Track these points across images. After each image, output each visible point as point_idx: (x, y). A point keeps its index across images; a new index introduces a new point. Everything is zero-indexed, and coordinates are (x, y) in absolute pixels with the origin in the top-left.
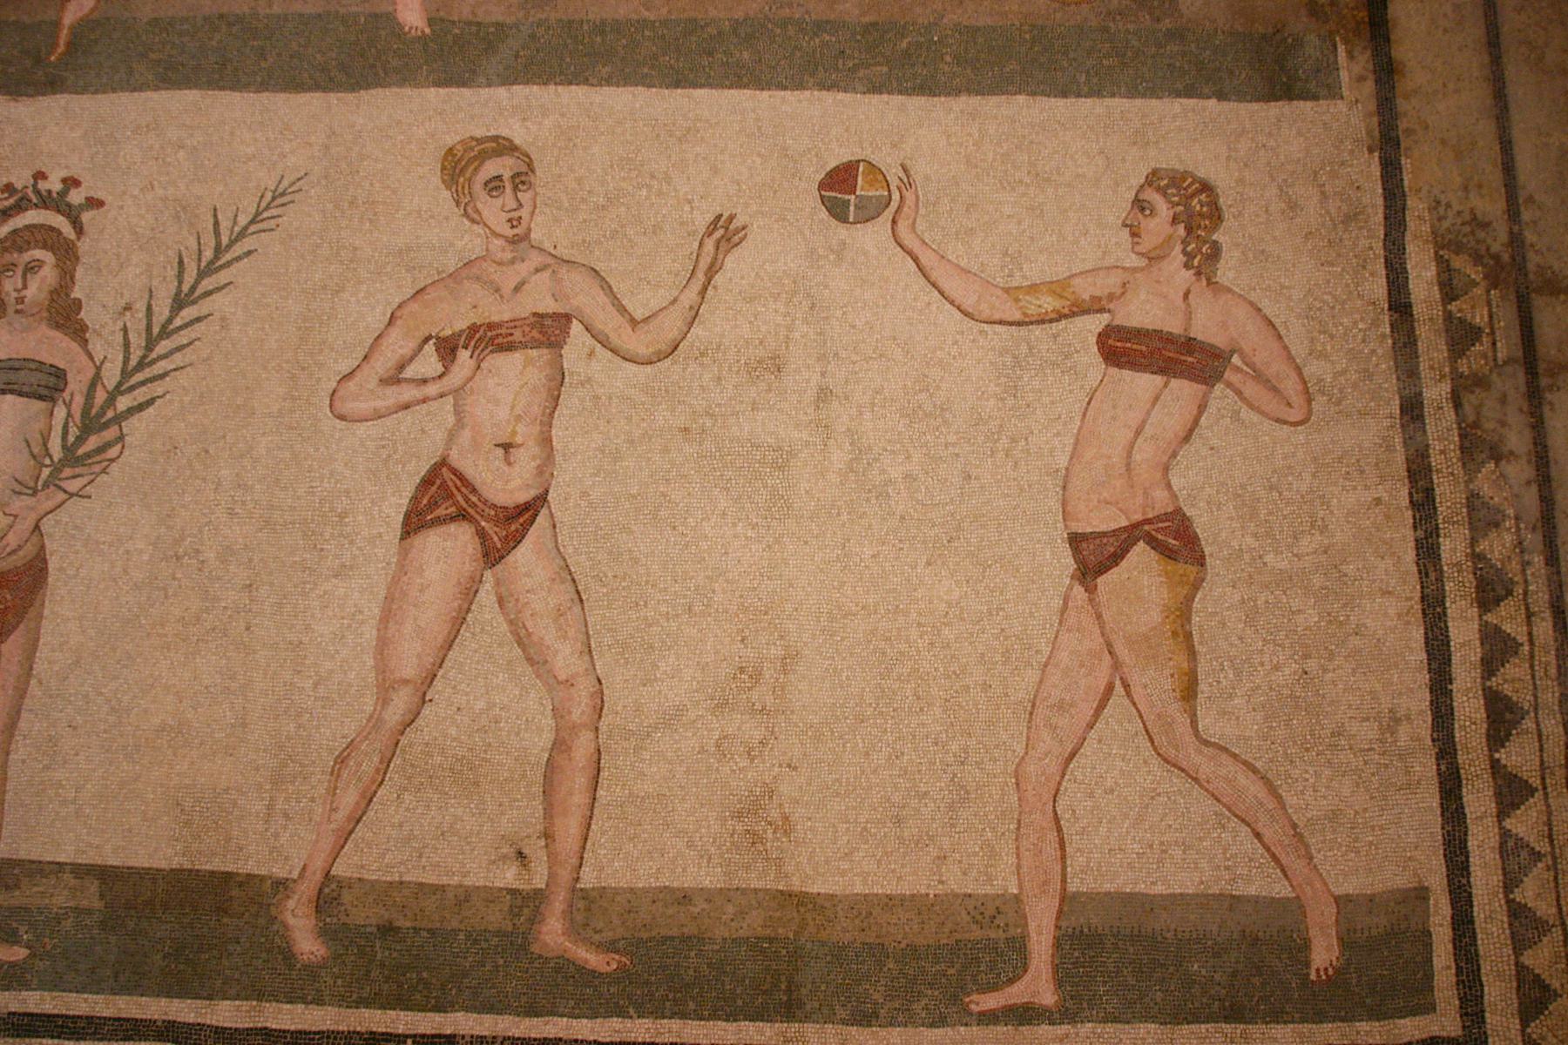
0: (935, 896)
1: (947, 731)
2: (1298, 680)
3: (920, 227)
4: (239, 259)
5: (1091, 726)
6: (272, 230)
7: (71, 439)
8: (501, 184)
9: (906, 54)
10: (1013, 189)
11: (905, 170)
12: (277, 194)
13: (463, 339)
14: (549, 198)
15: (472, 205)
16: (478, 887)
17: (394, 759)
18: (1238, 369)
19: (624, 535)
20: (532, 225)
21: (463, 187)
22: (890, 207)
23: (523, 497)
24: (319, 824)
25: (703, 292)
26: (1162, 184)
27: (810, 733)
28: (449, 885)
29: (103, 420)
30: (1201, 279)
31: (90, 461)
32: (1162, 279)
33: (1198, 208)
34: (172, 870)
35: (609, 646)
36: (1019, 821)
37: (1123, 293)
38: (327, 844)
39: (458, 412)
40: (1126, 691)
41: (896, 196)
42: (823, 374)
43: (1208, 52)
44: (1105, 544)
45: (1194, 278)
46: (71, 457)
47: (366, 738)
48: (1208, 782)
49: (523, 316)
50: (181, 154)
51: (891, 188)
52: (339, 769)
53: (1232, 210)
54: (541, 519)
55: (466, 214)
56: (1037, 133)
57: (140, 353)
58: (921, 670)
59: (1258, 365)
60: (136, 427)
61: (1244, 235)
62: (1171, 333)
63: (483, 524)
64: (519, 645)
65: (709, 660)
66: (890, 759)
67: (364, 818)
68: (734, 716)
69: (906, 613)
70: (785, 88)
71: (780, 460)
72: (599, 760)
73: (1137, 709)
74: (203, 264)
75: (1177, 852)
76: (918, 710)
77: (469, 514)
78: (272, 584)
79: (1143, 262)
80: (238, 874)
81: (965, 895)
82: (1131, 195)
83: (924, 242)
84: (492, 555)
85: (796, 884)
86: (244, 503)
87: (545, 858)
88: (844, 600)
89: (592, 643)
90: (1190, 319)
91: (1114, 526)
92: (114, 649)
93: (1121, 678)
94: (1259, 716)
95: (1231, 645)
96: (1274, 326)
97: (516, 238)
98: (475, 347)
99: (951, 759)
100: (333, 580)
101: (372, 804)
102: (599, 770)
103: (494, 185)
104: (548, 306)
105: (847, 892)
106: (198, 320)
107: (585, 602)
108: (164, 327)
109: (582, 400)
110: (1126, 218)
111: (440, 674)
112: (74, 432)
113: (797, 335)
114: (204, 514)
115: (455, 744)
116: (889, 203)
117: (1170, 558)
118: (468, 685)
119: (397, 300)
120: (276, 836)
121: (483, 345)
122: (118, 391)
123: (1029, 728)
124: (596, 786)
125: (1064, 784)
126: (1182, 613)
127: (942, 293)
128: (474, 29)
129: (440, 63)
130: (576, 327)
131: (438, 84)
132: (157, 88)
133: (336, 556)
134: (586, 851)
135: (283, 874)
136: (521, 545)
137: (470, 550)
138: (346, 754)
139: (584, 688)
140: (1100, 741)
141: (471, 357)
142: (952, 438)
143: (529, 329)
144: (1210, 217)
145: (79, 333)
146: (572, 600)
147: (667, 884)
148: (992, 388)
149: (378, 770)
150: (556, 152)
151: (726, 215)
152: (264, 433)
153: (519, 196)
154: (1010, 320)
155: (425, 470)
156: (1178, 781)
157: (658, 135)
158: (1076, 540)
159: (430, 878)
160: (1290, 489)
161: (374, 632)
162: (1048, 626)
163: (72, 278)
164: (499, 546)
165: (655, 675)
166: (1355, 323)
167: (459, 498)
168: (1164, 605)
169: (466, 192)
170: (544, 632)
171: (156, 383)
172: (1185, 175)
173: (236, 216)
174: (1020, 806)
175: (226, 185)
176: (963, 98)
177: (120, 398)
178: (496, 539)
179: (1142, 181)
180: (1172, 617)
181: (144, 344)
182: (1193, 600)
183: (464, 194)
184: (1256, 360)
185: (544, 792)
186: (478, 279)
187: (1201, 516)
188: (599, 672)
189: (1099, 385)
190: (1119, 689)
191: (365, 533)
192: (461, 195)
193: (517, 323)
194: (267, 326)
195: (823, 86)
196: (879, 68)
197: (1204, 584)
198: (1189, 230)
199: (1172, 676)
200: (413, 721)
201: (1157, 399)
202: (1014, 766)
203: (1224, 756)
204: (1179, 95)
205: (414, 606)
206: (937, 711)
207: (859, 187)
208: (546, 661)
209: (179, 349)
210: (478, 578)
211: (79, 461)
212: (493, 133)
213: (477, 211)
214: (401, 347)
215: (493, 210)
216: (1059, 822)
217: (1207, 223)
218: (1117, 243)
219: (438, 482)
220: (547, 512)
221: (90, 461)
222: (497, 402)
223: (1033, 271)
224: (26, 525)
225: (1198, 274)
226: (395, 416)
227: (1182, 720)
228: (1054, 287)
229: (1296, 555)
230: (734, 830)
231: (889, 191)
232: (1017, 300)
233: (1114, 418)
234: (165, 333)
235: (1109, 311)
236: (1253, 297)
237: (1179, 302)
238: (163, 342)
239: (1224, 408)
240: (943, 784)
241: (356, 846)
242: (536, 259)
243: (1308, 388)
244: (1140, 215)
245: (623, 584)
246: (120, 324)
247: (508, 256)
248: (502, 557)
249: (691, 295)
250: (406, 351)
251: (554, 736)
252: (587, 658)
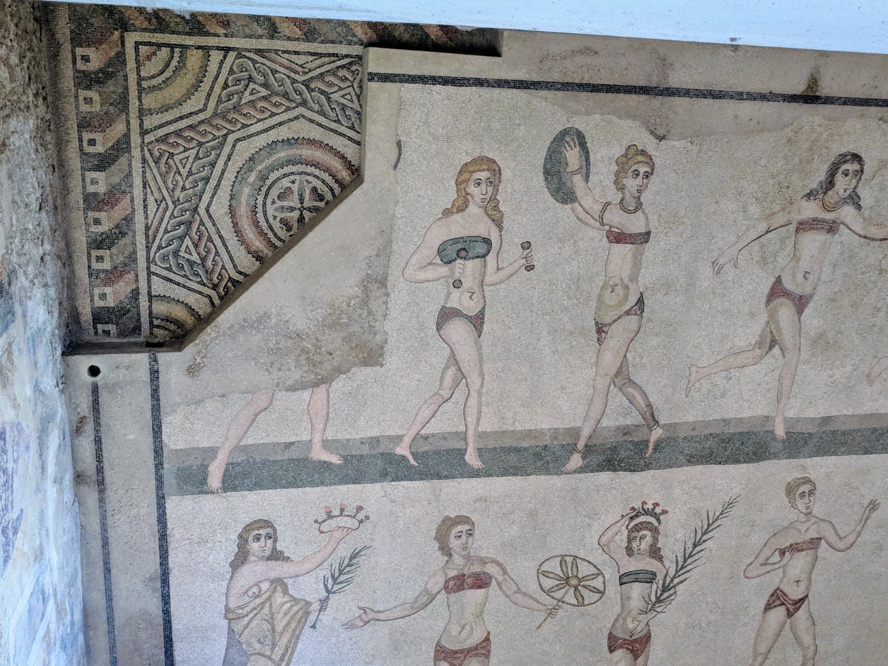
7: (658, 595)
23: (801, 597)
25: (863, 527)
39: (784, 572)
46: (659, 600)
54: (806, 602)
55: (792, 506)
60: (680, 588)
84: (790, 615)
103: (803, 495)
106: (702, 550)
108: (690, 554)
112: (659, 592)
122: (674, 577)
128: (801, 436)
130: (823, 541)
131: (787, 458)
145: (660, 559)
163: (657, 540)
186: (794, 528)
211: (661, 601)
215: (801, 504)
224: (643, 624)
234: (690, 556)
247: (805, 519)
249: (859, 528)
250: (769, 554)
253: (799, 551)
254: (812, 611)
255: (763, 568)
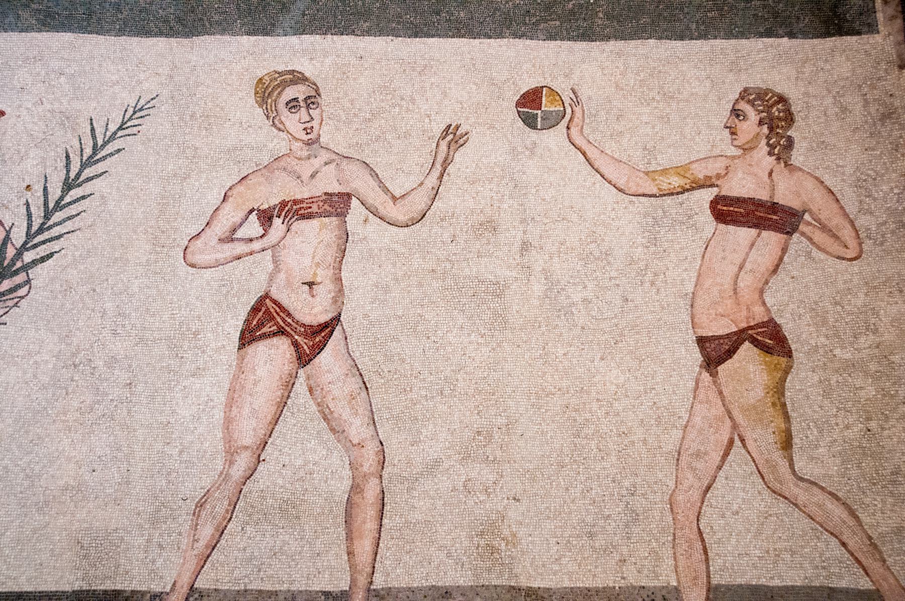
0: (619, 588)
1: (621, 473)
2: (864, 435)
3: (587, 130)
4: (111, 155)
5: (720, 468)
6: (135, 135)
8: (298, 104)
9: (572, 12)
10: (648, 104)
11: (574, 93)
12: (136, 109)
13: (276, 211)
14: (332, 114)
15: (278, 118)
16: (301, 592)
17: (239, 502)
18: (809, 224)
19: (394, 343)
20: (321, 133)
21: (271, 106)
22: (565, 118)
24: (186, 551)
26: (751, 98)
27: (527, 476)
28: (280, 591)
29: (14, 269)
30: (780, 163)
31: (4, 298)
32: (753, 163)
33: (777, 114)
34: (74, 591)
35: (387, 419)
36: (674, 534)
37: (726, 174)
38: (192, 565)
39: (275, 261)
40: (742, 443)
41: (569, 111)
42: (525, 232)
43: (781, 5)
44: (722, 344)
45: (775, 162)
47: (218, 488)
48: (805, 506)
49: (318, 195)
50: (63, 79)
51: (565, 105)
52: (200, 511)
53: (800, 114)
54: (337, 333)
55: (274, 124)
56: (664, 66)
57: (40, 221)
58: (601, 431)
59: (823, 220)
60: (39, 274)
61: (809, 131)
62: (761, 200)
63: (296, 337)
64: (324, 420)
65: (456, 427)
66: (583, 492)
67: (218, 545)
68: (475, 465)
69: (588, 393)
70: (490, 37)
71: (498, 291)
72: (383, 498)
73: (751, 456)
74: (85, 158)
75: (787, 557)
76: (600, 458)
77: (286, 331)
78: (146, 383)
79: (739, 152)
80: (125, 591)
81: (640, 587)
82: (729, 107)
83: (589, 141)
84: (304, 359)
85: (524, 582)
86: (123, 326)
87: (348, 569)
88: (546, 384)
89: (375, 417)
90: (774, 189)
91: (727, 331)
92: (27, 432)
93: (739, 435)
94: (838, 461)
95: (814, 411)
96: (832, 193)
97: (310, 141)
98: (286, 217)
99: (625, 492)
100: (191, 378)
101: (224, 535)
102: (383, 505)
103: (293, 104)
104: (335, 188)
105: (559, 586)
106: (83, 198)
107: (369, 389)
108: (57, 203)
109: (361, 252)
110: (727, 122)
111: (269, 442)
113: (505, 206)
114: (94, 335)
115: (282, 490)
116: (564, 116)
117: (767, 352)
118: (290, 449)
119: (229, 185)
120: (154, 562)
121: (290, 215)
122: (24, 248)
123: (677, 470)
124: (382, 516)
125: (704, 508)
126: (779, 390)
127: (603, 176)
129: (249, 18)
130: (354, 202)
131: (249, 33)
132: (40, 31)
133: (192, 362)
134: (377, 562)
135: (158, 589)
136: (323, 351)
137: (288, 356)
138: (203, 500)
139: (371, 449)
140: (726, 478)
141: (283, 223)
142: (614, 274)
143: (322, 204)
144: (785, 120)
146: (360, 388)
147: (434, 584)
148: (640, 240)
149: (227, 511)
150: (335, 82)
151: (454, 125)
152: (136, 277)
153: (310, 112)
154: (650, 193)
155: (254, 301)
156: (783, 505)
157: (405, 70)
158: (702, 341)
159: (268, 587)
160: (850, 304)
161: (222, 414)
162: (686, 400)
164: (308, 352)
165: (420, 438)
166: (892, 189)
167: (279, 320)
168: (765, 385)
169: (273, 109)
170: (342, 410)
171: (54, 242)
172: (767, 91)
173: (107, 124)
174: (674, 524)
175: (98, 102)
176: (612, 42)
177: (25, 253)
178: (305, 347)
179: (737, 96)
180: (771, 392)
181: (43, 215)
182: (785, 381)
183: (272, 110)
184: (822, 217)
185: (346, 522)
187: (787, 324)
188: (381, 437)
189: (713, 236)
190: (737, 442)
191: (213, 345)
192: (269, 111)
193: (314, 200)
194: (135, 202)
195: (516, 36)
196: (553, 23)
197: (792, 370)
198: (771, 129)
199: (774, 433)
200: (252, 475)
201: (753, 245)
202: (668, 496)
203: (815, 488)
204: (761, 35)
205: (250, 395)
206: (614, 459)
207: (543, 105)
208: (344, 431)
209: (69, 218)
210: (294, 375)
212: (290, 68)
213: (282, 123)
214: (232, 217)
215: (293, 122)
216: (702, 535)
217: (783, 123)
218: (721, 140)
219: (263, 309)
220: (341, 328)
221: (4, 298)
222: (302, 254)
223: (663, 161)
225: (778, 159)
226: (231, 264)
227: (783, 466)
228: (679, 170)
229: (856, 349)
230: (478, 544)
231: (564, 107)
232: (654, 180)
233: (724, 258)
234: (59, 206)
235: (717, 186)
236: (818, 174)
237: (766, 178)
238: (57, 214)
239: (800, 250)
240: (620, 510)
241: (213, 565)
242: (324, 156)
243: (858, 235)
244: (736, 120)
245: (395, 376)
246: (23, 201)
247: (305, 153)
248: (311, 360)
249: (432, 180)
250: (237, 219)
251: (351, 482)
252: (372, 428)
253: (304, 217)
254: (356, 355)
255: (227, 246)
